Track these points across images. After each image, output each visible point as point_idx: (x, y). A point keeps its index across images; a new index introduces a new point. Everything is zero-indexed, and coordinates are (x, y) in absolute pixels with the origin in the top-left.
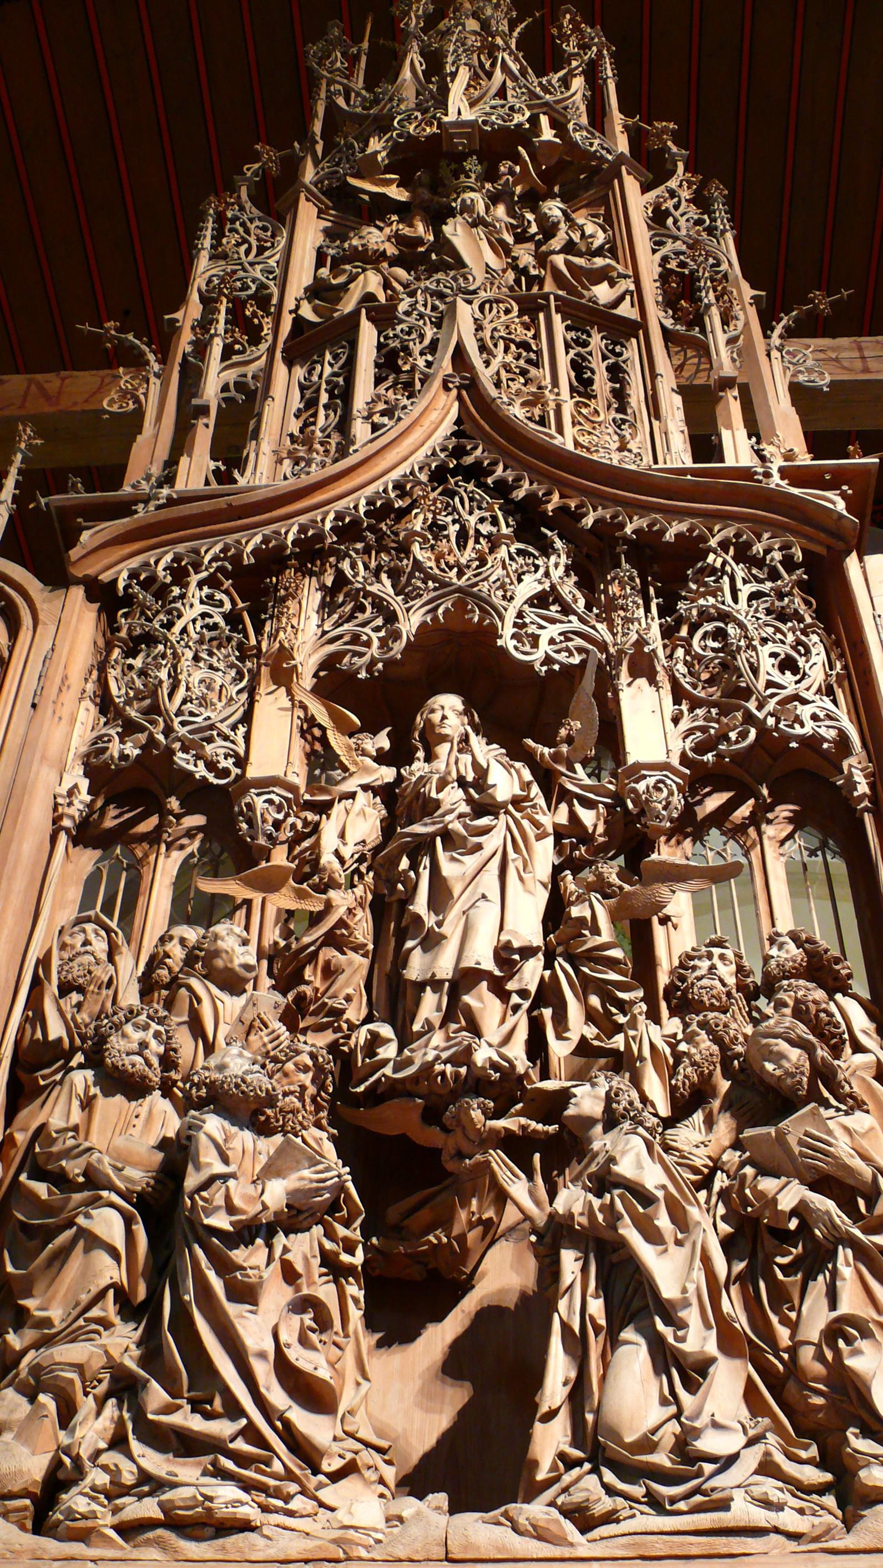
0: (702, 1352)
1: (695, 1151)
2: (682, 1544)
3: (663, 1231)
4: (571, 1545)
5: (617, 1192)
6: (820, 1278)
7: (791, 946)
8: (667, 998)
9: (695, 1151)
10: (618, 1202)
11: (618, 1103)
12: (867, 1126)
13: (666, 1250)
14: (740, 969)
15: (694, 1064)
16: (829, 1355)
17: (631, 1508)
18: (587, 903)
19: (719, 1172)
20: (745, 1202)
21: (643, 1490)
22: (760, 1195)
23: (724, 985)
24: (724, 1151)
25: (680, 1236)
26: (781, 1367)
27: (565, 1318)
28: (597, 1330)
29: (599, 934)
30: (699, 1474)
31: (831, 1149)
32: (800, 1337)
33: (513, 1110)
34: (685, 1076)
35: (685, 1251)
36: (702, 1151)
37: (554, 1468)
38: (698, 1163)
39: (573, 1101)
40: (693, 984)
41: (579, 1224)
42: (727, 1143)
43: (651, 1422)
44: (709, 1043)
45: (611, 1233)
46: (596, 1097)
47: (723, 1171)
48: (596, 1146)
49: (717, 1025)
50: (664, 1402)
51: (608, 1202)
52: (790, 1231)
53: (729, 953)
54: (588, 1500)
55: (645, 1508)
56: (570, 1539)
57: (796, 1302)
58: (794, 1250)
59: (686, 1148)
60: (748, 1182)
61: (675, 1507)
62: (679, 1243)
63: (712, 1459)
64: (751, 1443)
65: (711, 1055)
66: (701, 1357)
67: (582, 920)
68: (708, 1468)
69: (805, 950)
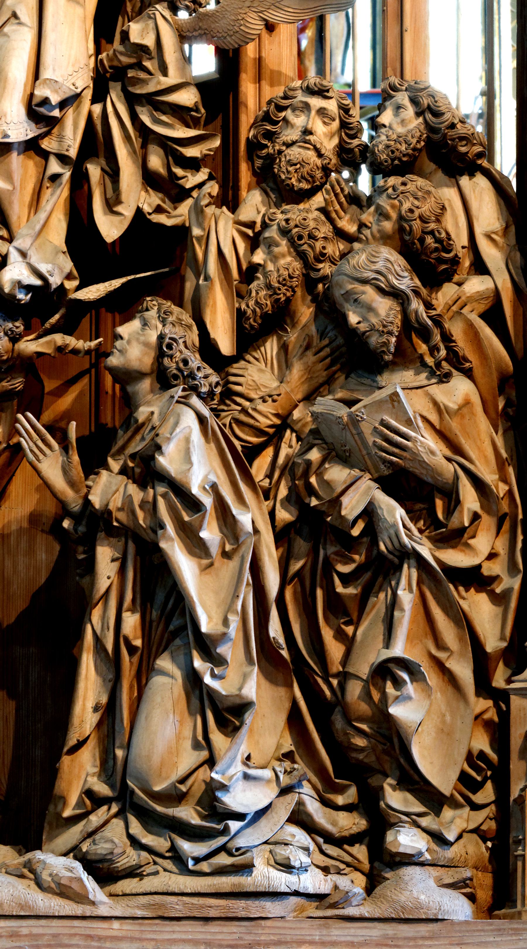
0: (239, 696)
1: (261, 407)
2: (202, 907)
3: (209, 544)
4: (93, 903)
5: (161, 489)
6: (382, 596)
7: (410, 111)
8: (250, 159)
9: (261, 407)
10: (161, 504)
11: (171, 357)
12: (459, 399)
13: (211, 565)
14: (344, 125)
15: (269, 286)
16: (376, 696)
17: (155, 863)
18: (151, 23)
19: (288, 432)
20: (311, 491)
21: (168, 844)
22: (327, 485)
23: (320, 155)
24: (296, 406)
25: (228, 548)
26: (328, 693)
27: (98, 632)
28: (132, 650)
29: (165, 73)
30: (226, 831)
31: (409, 444)
32: (350, 669)
33: (47, 325)
34: (257, 303)
35: (233, 565)
36: (267, 408)
37: (80, 803)
38: (263, 422)
39: (118, 344)
40: (280, 152)
41: (117, 520)
42: (300, 396)
43: (182, 770)
44: (289, 259)
45: (152, 535)
46: (146, 344)
47: (293, 430)
48: (142, 413)
49: (300, 237)
50: (197, 746)
51: (151, 499)
52: (352, 536)
53: (332, 106)
54: (112, 853)
55: (168, 864)
56: (91, 897)
57: (355, 617)
58: (356, 557)
59: (253, 395)
60: (314, 468)
61: (198, 868)
62: (226, 555)
63: (240, 817)
64: (285, 791)
65: (291, 277)
66: (238, 701)
67: (143, 49)
68: (234, 825)
69: (425, 119)
